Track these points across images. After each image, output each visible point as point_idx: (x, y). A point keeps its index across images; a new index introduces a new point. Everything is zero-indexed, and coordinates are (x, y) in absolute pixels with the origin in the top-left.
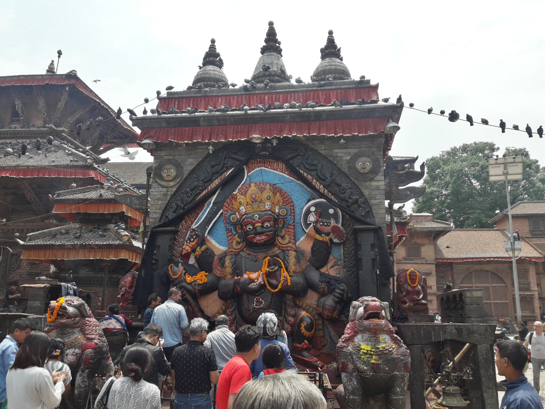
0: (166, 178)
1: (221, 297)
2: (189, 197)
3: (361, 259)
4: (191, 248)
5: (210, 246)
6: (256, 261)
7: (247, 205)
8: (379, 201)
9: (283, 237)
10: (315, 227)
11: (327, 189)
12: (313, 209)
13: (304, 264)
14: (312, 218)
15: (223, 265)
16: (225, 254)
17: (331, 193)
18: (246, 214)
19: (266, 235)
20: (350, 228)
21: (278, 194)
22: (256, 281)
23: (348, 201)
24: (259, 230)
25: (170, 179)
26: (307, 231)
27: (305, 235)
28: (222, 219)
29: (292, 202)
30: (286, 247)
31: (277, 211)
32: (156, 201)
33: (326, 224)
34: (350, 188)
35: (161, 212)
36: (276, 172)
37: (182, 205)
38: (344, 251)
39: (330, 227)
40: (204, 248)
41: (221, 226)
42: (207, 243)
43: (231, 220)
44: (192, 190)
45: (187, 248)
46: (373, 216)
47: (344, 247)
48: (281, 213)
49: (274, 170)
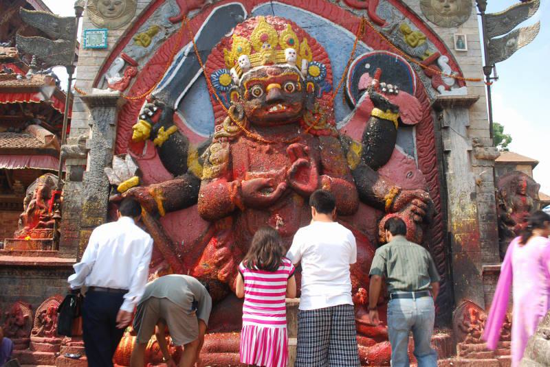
0: (106, 14)
2: (144, 46)
3: (448, 152)
5: (183, 129)
7: (251, 53)
8: (474, 59)
21: (305, 40)
23: (421, 59)
25: (115, 15)
27: (352, 114)
28: (203, 84)
29: (327, 56)
31: (304, 67)
33: (391, 91)
34: (425, 39)
36: (297, 8)
37: (134, 59)
38: (418, 140)
40: (172, 129)
43: (221, 82)
44: (152, 35)
47: (418, 133)
49: (294, 5)
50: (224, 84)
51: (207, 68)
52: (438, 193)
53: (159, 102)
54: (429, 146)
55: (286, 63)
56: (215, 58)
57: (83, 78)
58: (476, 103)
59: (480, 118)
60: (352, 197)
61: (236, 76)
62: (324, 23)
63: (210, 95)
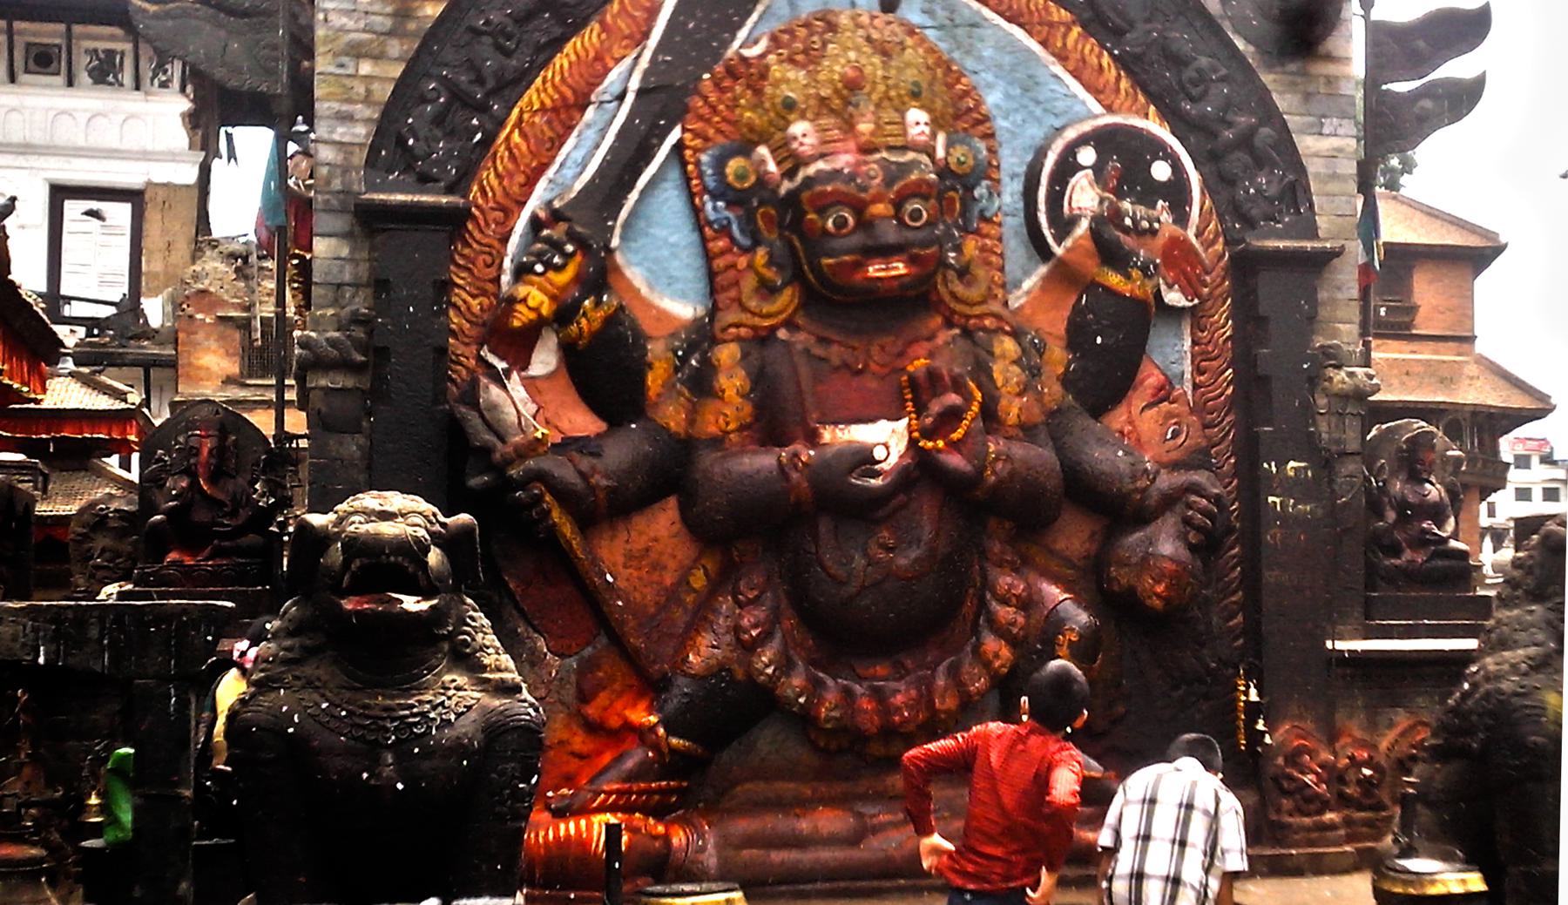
1: (696, 526)
2: (508, 54)
4: (553, 298)
6: (860, 372)
9: (964, 273)
10: (1095, 233)
11: (1131, 73)
12: (1087, 156)
13: (1052, 390)
14: (1084, 196)
15: (701, 384)
16: (702, 336)
17: (1146, 92)
18: (822, 156)
19: (912, 261)
20: (1219, 247)
22: (879, 453)
23: (1214, 135)
24: (889, 233)
26: (1059, 251)
27: (1043, 269)
29: (986, 119)
30: (976, 316)
31: (940, 154)
32: (345, 60)
33: (1145, 224)
34: (1223, 80)
35: (376, 116)
38: (1194, 343)
39: (1160, 240)
41: (670, 204)
42: (612, 279)
43: (731, 178)
45: (536, 298)
46: (1312, 206)
47: (1197, 327)
48: (953, 167)
50: (738, 185)
51: (688, 136)
52: (1235, 475)
53: (579, 229)
54: (1220, 361)
55: (904, 148)
56: (705, 111)
57: (336, 137)
58: (1335, 261)
59: (1340, 296)
60: (1053, 483)
61: (772, 167)
62: (978, 19)
63: (696, 211)
